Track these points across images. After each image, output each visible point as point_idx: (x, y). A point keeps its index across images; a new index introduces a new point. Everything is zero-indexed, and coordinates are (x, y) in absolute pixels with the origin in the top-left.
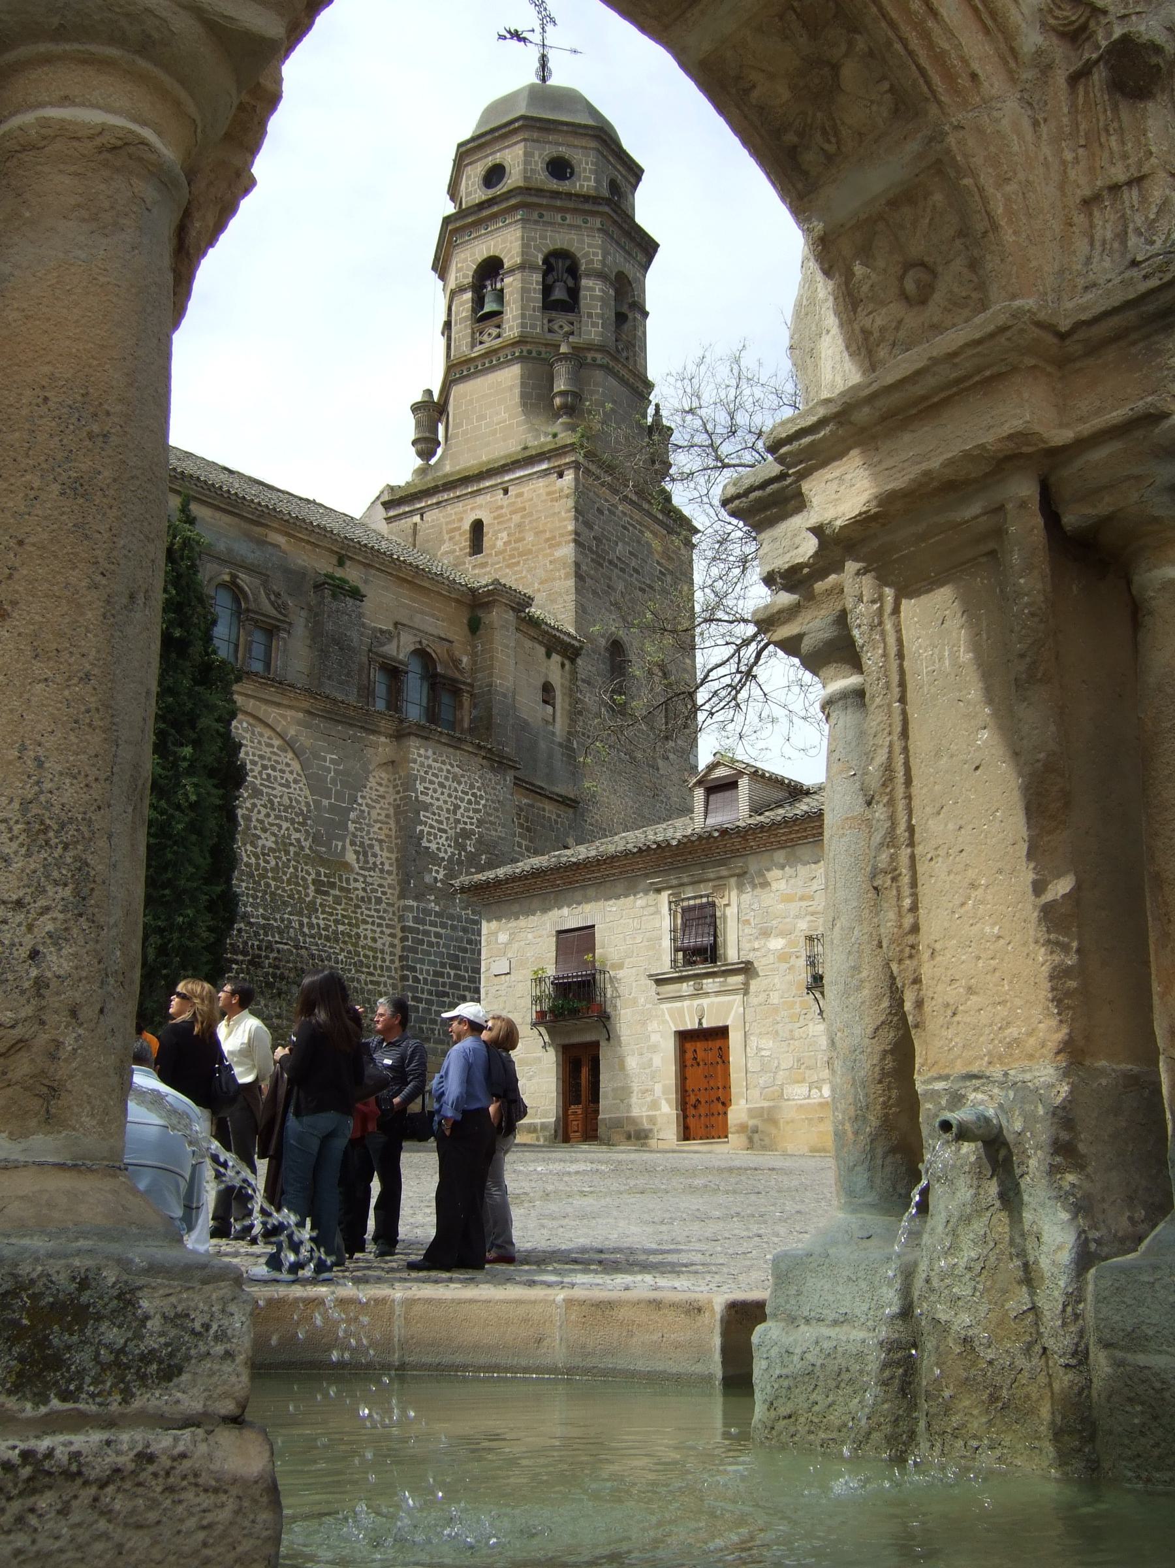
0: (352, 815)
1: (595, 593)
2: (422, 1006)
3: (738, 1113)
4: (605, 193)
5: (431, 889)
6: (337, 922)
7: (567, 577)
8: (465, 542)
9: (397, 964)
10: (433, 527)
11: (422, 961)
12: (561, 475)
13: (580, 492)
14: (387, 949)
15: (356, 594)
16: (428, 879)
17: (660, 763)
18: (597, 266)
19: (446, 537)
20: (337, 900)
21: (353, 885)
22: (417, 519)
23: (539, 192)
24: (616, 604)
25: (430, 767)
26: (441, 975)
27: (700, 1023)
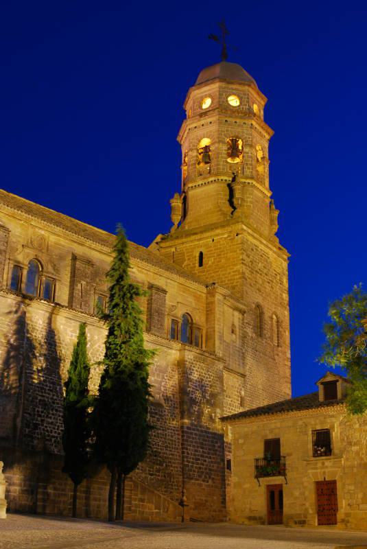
0: (163, 384)
1: (251, 285)
2: (190, 464)
3: (341, 515)
9: (180, 447)
10: (181, 254)
11: (190, 446)
15: (165, 292)
17: (276, 357)
19: (187, 258)
20: (158, 420)
22: (173, 250)
24: (258, 289)
25: (192, 363)
27: (325, 479)
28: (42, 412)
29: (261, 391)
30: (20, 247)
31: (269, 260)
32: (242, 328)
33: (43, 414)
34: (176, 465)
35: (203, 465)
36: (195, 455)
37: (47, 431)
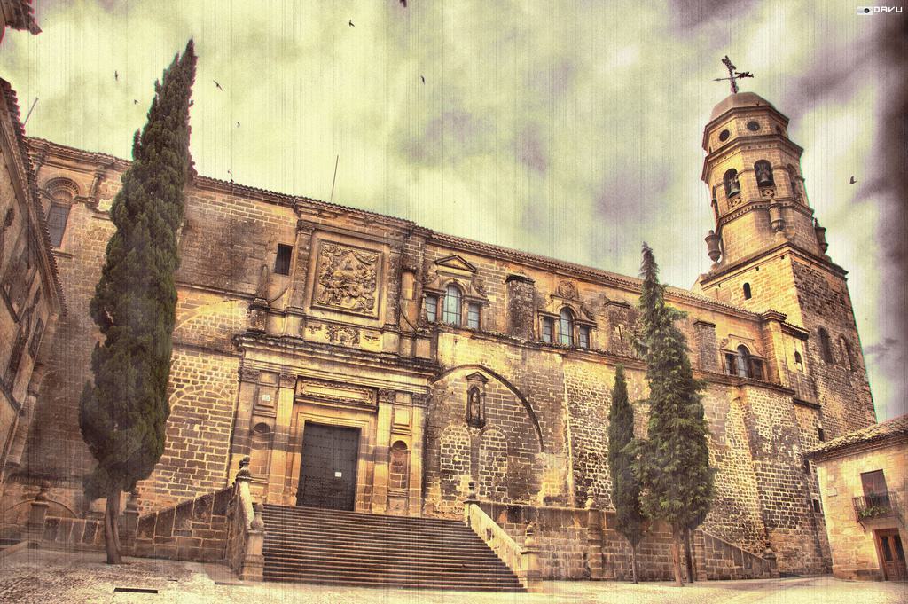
0: (726, 424)
1: (808, 308)
4: (775, 132)
5: (766, 455)
6: (728, 474)
7: (795, 302)
8: (742, 294)
11: (768, 489)
12: (783, 258)
13: (793, 265)
14: (751, 485)
16: (764, 450)
17: (852, 383)
18: (779, 164)
21: (732, 456)
22: (717, 287)
23: (747, 138)
24: (818, 312)
26: (777, 494)
28: (594, 467)
29: (841, 422)
30: (547, 297)
31: (824, 280)
32: (808, 355)
33: (594, 469)
34: (754, 512)
35: (787, 509)
36: (775, 499)
37: (602, 486)
